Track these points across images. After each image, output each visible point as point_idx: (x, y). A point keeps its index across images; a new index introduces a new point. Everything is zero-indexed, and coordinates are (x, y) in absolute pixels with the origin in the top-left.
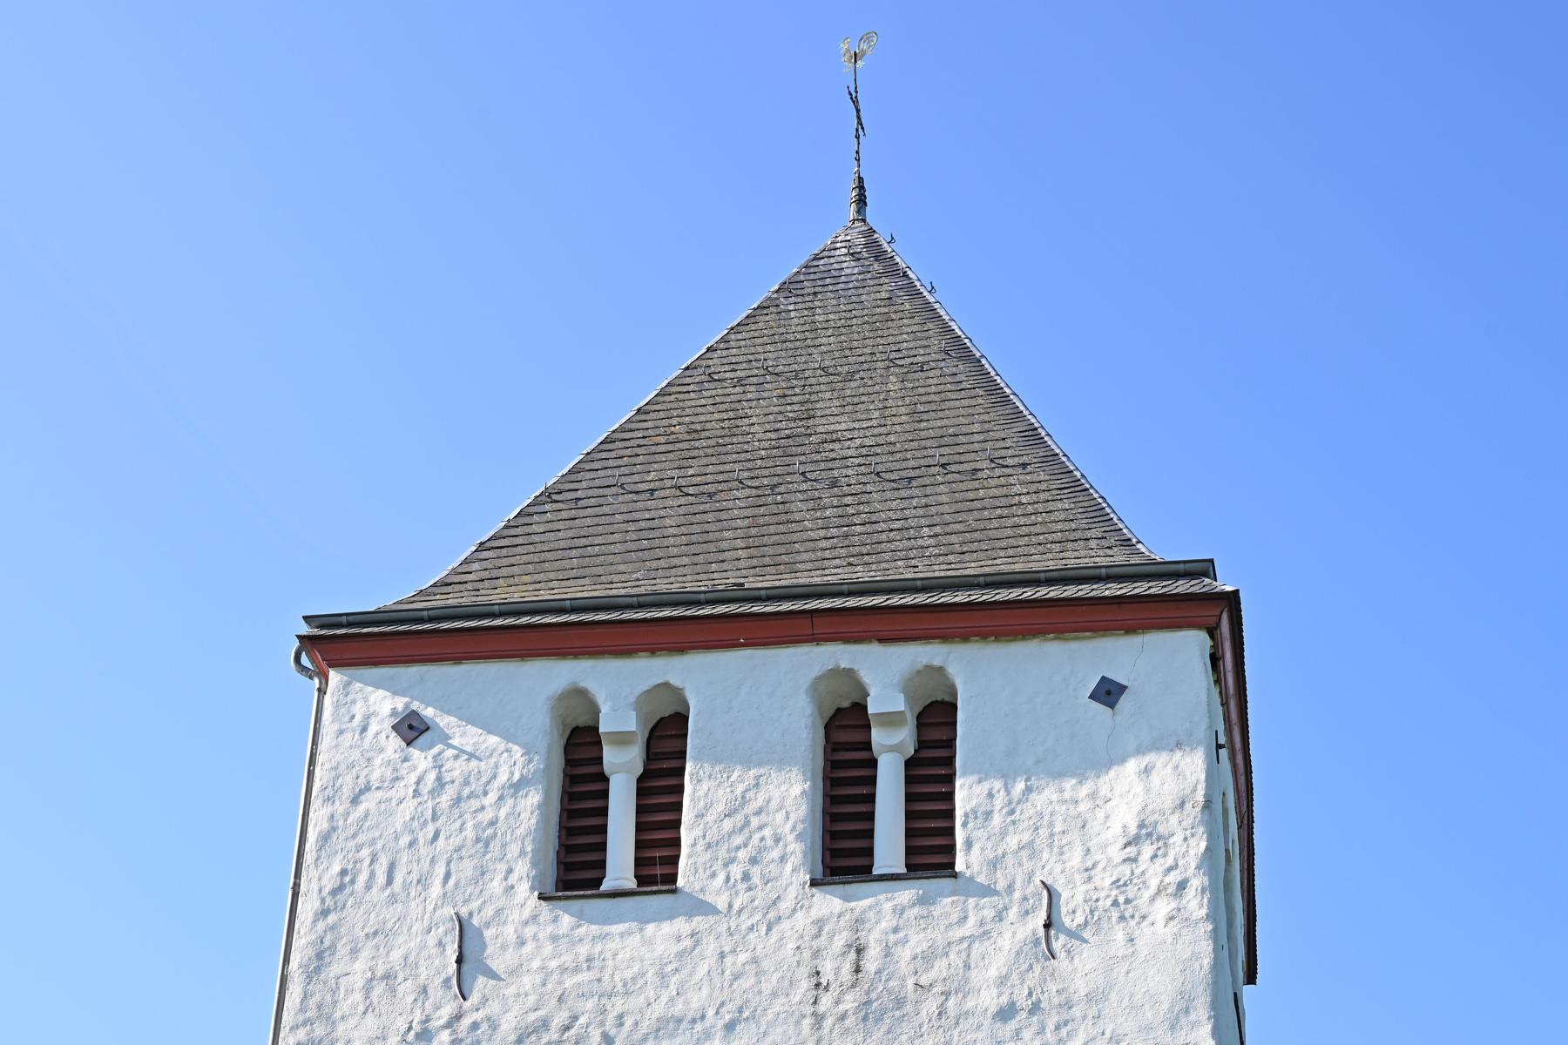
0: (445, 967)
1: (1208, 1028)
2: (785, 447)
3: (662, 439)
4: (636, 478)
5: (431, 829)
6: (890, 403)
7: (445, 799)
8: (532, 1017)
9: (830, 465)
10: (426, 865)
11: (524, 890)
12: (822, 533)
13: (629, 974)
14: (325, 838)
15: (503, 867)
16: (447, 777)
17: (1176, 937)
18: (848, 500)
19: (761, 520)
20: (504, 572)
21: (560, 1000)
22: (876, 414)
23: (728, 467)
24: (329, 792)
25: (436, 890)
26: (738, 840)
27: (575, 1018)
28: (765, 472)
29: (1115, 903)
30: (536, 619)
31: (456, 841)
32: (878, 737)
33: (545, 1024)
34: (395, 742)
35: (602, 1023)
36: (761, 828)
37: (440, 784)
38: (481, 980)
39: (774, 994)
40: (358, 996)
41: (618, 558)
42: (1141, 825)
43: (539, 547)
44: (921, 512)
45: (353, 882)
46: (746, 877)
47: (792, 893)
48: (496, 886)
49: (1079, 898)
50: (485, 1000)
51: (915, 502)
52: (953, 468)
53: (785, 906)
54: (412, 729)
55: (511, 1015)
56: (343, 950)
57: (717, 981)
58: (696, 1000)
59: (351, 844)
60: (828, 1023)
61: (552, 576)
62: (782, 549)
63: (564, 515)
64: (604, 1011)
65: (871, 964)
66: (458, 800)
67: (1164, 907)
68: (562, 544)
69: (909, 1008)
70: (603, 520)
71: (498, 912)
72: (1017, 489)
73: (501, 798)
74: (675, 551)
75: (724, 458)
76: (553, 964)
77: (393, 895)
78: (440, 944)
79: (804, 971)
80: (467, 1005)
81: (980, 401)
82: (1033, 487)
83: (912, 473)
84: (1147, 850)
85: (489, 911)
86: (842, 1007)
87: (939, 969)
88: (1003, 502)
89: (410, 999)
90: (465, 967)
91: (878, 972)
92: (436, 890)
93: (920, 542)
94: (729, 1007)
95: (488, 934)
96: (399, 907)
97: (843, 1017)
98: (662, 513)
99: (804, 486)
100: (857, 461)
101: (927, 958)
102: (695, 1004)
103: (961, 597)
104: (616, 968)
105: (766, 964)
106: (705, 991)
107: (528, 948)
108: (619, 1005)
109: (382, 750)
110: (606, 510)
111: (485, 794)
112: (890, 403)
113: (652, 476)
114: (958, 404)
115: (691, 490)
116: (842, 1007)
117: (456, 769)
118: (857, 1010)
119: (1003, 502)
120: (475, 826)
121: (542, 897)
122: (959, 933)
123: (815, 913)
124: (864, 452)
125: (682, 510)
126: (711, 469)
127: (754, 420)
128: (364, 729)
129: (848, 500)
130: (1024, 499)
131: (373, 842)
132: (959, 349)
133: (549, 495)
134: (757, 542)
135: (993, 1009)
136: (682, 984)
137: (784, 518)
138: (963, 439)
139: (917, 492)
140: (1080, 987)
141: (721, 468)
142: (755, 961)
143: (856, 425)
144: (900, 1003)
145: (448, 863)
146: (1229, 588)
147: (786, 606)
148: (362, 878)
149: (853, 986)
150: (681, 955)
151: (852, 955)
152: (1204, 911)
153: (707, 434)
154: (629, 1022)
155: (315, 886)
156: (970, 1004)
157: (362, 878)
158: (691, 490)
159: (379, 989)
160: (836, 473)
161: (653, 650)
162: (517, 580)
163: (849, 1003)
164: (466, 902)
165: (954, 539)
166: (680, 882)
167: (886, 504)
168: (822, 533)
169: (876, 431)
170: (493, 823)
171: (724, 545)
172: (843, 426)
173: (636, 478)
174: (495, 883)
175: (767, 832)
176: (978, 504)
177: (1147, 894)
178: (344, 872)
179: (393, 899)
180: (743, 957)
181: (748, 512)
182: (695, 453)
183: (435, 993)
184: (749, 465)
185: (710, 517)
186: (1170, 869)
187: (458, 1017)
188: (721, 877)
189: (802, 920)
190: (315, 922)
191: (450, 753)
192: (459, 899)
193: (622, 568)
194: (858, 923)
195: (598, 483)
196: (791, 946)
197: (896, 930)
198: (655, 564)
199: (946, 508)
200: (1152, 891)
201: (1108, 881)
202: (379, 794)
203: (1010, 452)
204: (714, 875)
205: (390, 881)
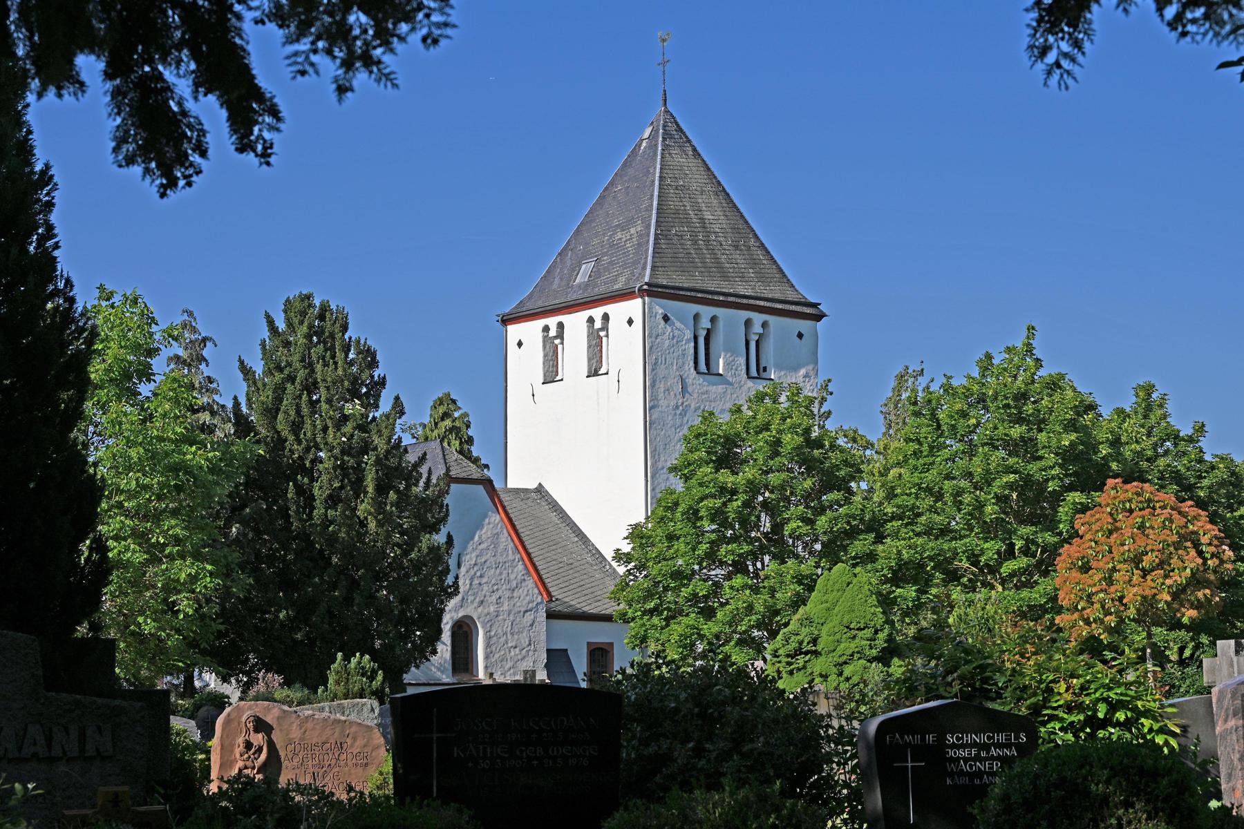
14: (651, 348)
25: (675, 368)
34: (662, 322)
37: (674, 337)
54: (666, 318)
66: (677, 342)
92: (675, 368)
142: (737, 397)
179: (666, 368)
183: (678, 397)
187: (683, 403)
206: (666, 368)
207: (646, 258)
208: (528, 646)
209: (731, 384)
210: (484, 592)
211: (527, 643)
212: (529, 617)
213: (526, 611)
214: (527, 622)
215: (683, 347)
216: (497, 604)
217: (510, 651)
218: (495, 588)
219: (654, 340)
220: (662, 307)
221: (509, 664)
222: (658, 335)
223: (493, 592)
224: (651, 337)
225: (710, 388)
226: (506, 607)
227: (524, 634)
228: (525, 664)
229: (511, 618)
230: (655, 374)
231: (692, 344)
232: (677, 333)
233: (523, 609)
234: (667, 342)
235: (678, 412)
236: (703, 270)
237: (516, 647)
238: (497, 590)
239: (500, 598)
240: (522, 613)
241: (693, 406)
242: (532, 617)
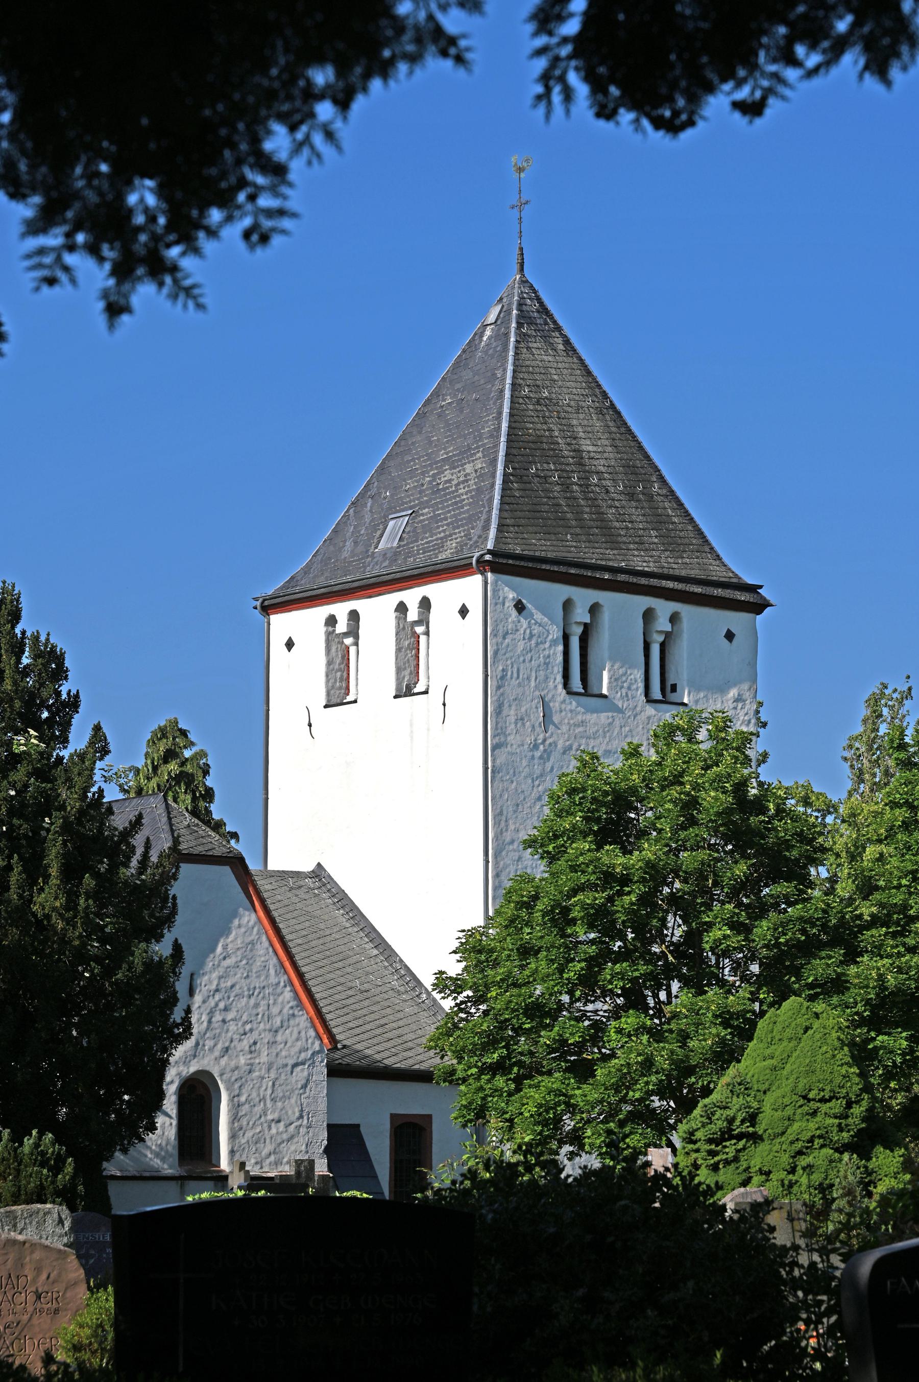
5: (529, 655)
7: (533, 642)
8: (568, 743)
14: (496, 653)
15: (553, 677)
25: (533, 684)
37: (531, 636)
38: (551, 726)
40: (513, 726)
47: (640, 704)
50: (552, 734)
53: (638, 709)
56: (506, 705)
59: (504, 657)
66: (537, 644)
71: (553, 696)
73: (551, 646)
76: (572, 722)
77: (519, 683)
78: (537, 708)
85: (550, 696)
92: (533, 684)
95: (551, 704)
107: (563, 713)
120: (544, 656)
136: (610, 737)
142: (631, 731)
148: (509, 673)
157: (509, 673)
178: (503, 670)
180: (627, 729)
183: (538, 729)
187: (544, 740)
191: (533, 621)
202: (511, 636)
205: (518, 677)
206: (519, 685)
207: (490, 512)
208: (298, 1119)
209: (620, 711)
210: (230, 1034)
211: (297, 1114)
212: (301, 1073)
213: (295, 1065)
214: (297, 1081)
215: (547, 652)
216: (251, 1052)
217: (270, 1128)
218: (248, 1027)
219: (500, 640)
220: (513, 589)
221: (269, 1147)
222: (507, 633)
223: (245, 1034)
224: (495, 635)
225: (588, 717)
226: (264, 1058)
227: (293, 1101)
228: (293, 1148)
229: (273, 1075)
230: (502, 694)
231: (560, 648)
232: (536, 630)
233: (291, 1062)
234: (521, 645)
235: (537, 754)
236: (578, 530)
237: (279, 1121)
238: (251, 1030)
239: (255, 1043)
240: (289, 1068)
242: (306, 1073)
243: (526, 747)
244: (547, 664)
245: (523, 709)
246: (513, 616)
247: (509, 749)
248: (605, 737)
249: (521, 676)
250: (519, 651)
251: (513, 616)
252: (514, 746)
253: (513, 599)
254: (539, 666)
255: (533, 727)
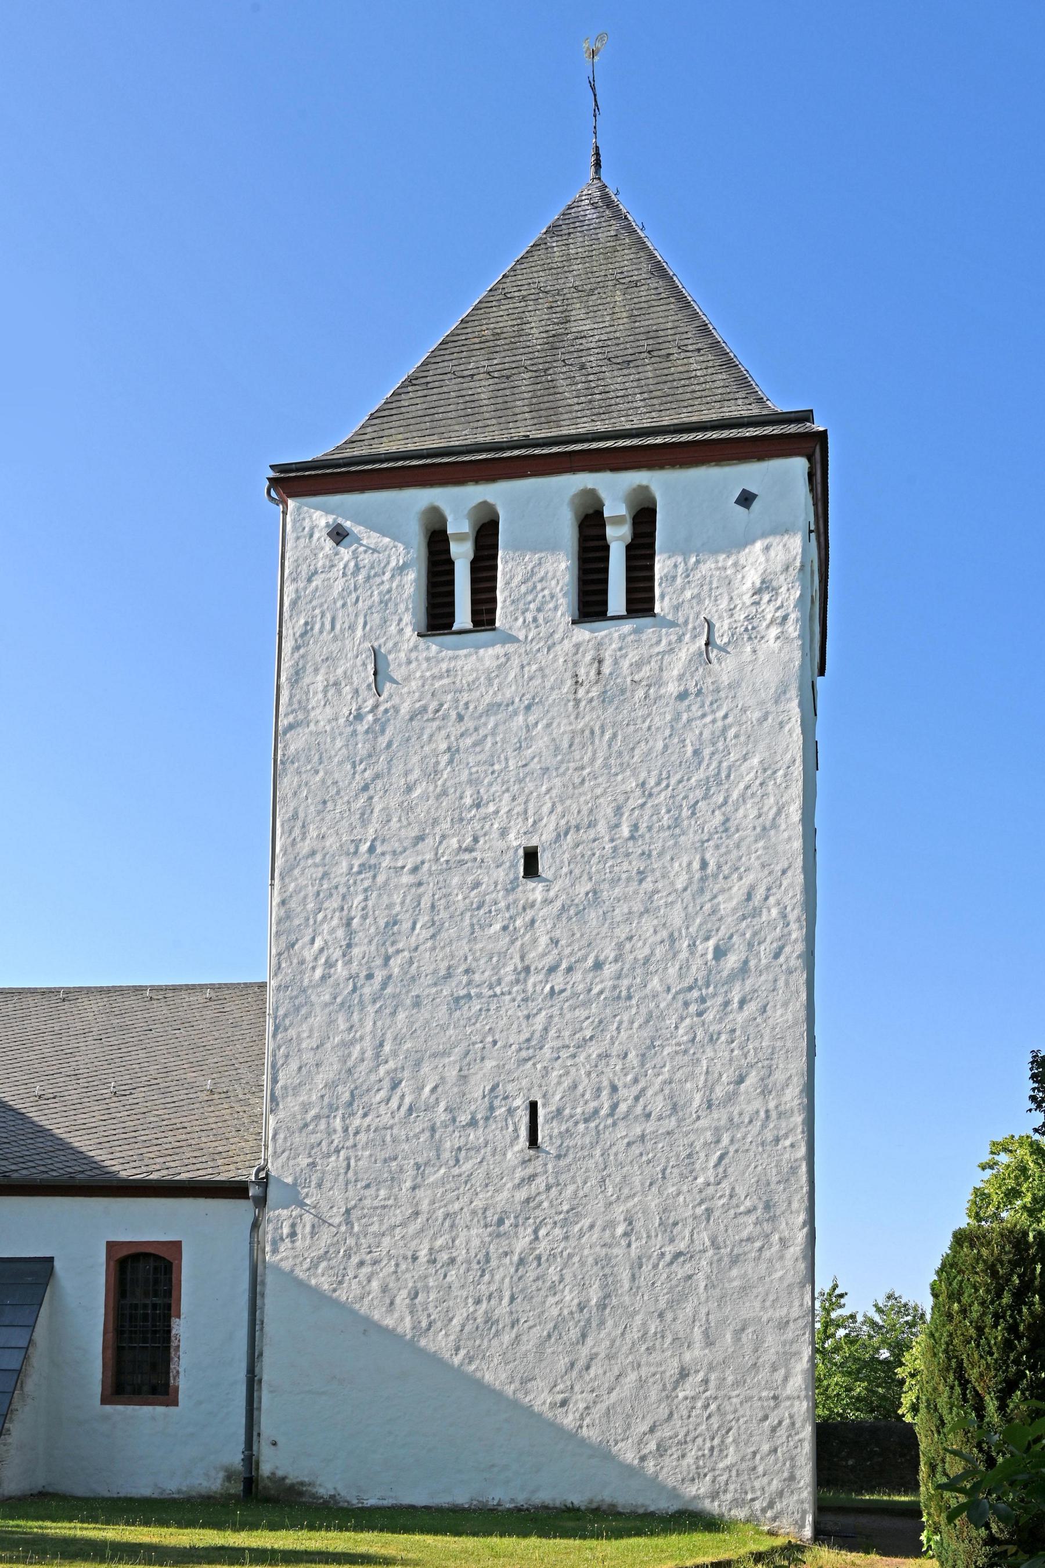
0: (368, 677)
1: (796, 702)
2: (553, 342)
3: (477, 340)
4: (463, 367)
5: (354, 596)
6: (617, 310)
7: (361, 578)
8: (418, 705)
9: (580, 354)
10: (352, 617)
11: (408, 631)
12: (576, 400)
13: (470, 679)
14: (294, 603)
15: (397, 618)
16: (361, 564)
17: (780, 650)
18: (591, 378)
19: (539, 393)
20: (386, 433)
21: (433, 695)
22: (608, 318)
23: (518, 358)
24: (294, 575)
25: (359, 633)
26: (530, 598)
27: (441, 705)
28: (541, 360)
29: (746, 630)
30: (407, 463)
31: (369, 603)
32: (610, 532)
33: (424, 709)
34: (329, 544)
35: (457, 708)
36: (543, 590)
37: (357, 568)
38: (388, 685)
39: (552, 689)
40: (320, 696)
41: (453, 421)
42: (763, 582)
43: (407, 416)
44: (635, 384)
45: (312, 629)
46: (535, 620)
48: (393, 629)
49: (726, 627)
50: (391, 696)
51: (632, 378)
52: (655, 353)
53: (557, 636)
54: (339, 535)
55: (406, 705)
56: (310, 669)
57: (520, 681)
58: (508, 693)
59: (309, 607)
60: (583, 704)
61: (415, 434)
62: (552, 412)
63: (420, 394)
64: (457, 701)
65: (606, 669)
66: (368, 578)
67: (774, 631)
68: (420, 413)
69: (628, 694)
70: (444, 396)
71: (396, 644)
72: (695, 366)
73: (393, 576)
74: (487, 415)
75: (515, 352)
76: (428, 674)
78: (364, 664)
79: (569, 674)
80: (382, 698)
81: (672, 306)
82: (704, 365)
83: (630, 358)
84: (766, 597)
85: (390, 644)
86: (590, 695)
87: (645, 671)
88: (686, 375)
89: (349, 696)
90: (379, 678)
91: (611, 674)
92: (359, 633)
93: (635, 405)
94: (528, 696)
95: (391, 657)
96: (339, 643)
97: (591, 700)
98: (479, 390)
99: (565, 369)
100: (596, 351)
101: (638, 665)
102: (508, 695)
103: (659, 440)
104: (463, 675)
105: (547, 671)
106: (513, 688)
107: (414, 665)
108: (465, 697)
109: (322, 549)
110: (445, 389)
111: (384, 573)
112: (617, 310)
113: (472, 366)
114: (658, 309)
115: (496, 374)
116: (590, 695)
117: (366, 559)
118: (599, 696)
119: (686, 375)
120: (379, 594)
121: (419, 635)
122: (657, 649)
123: (575, 640)
124: (600, 344)
125: (491, 388)
126: (507, 359)
127: (533, 325)
128: (311, 536)
129: (591, 378)
130: (699, 373)
131: (321, 605)
132: (660, 270)
133: (411, 381)
134: (537, 407)
135: (675, 694)
136: (500, 684)
137: (552, 391)
138: (661, 333)
139: (633, 371)
140: (725, 680)
141: (514, 359)
142: (541, 669)
143: (596, 326)
144: (623, 691)
145: (365, 617)
146: (821, 429)
147: (555, 449)
148: (317, 627)
149: (597, 683)
150: (499, 667)
151: (596, 665)
152: (796, 634)
153: (504, 336)
154: (471, 707)
155: (291, 632)
156: (662, 691)
157: (317, 627)
158: (496, 374)
159: (332, 691)
160: (583, 360)
161: (477, 480)
162: (394, 437)
163: (594, 694)
164: (377, 639)
165: (655, 401)
166: (497, 624)
167: (615, 380)
168: (576, 400)
169: (608, 330)
170: (389, 591)
171: (517, 410)
172: (588, 327)
173: (463, 367)
174: (393, 627)
175: (546, 592)
176: (670, 378)
177: (764, 624)
178: (306, 624)
179: (335, 639)
180: (534, 667)
181: (530, 388)
182: (498, 349)
183: (364, 693)
184: (531, 356)
185: (508, 392)
186: (778, 608)
187: (376, 707)
188: (521, 620)
189: (567, 645)
190: (292, 653)
191: (362, 549)
192: (373, 637)
193: (456, 428)
194: (599, 646)
195: (439, 371)
196: (561, 660)
197: (620, 649)
198: (476, 424)
199: (651, 381)
200: (768, 622)
201: (742, 617)
202: (323, 576)
203: (690, 341)
204: (516, 619)
205: (333, 628)
206: (335, 639)
220: (328, 511)
224: (294, 580)
234: (339, 586)
235: (362, 728)
241: (405, 709)
243: (342, 721)
244: (385, 603)
245: (340, 671)
246: (327, 549)
247: (312, 727)
248: (491, 684)
249: (338, 627)
250: (335, 594)
251: (327, 549)
252: (322, 723)
253: (327, 525)
254: (370, 608)
255: (357, 691)
